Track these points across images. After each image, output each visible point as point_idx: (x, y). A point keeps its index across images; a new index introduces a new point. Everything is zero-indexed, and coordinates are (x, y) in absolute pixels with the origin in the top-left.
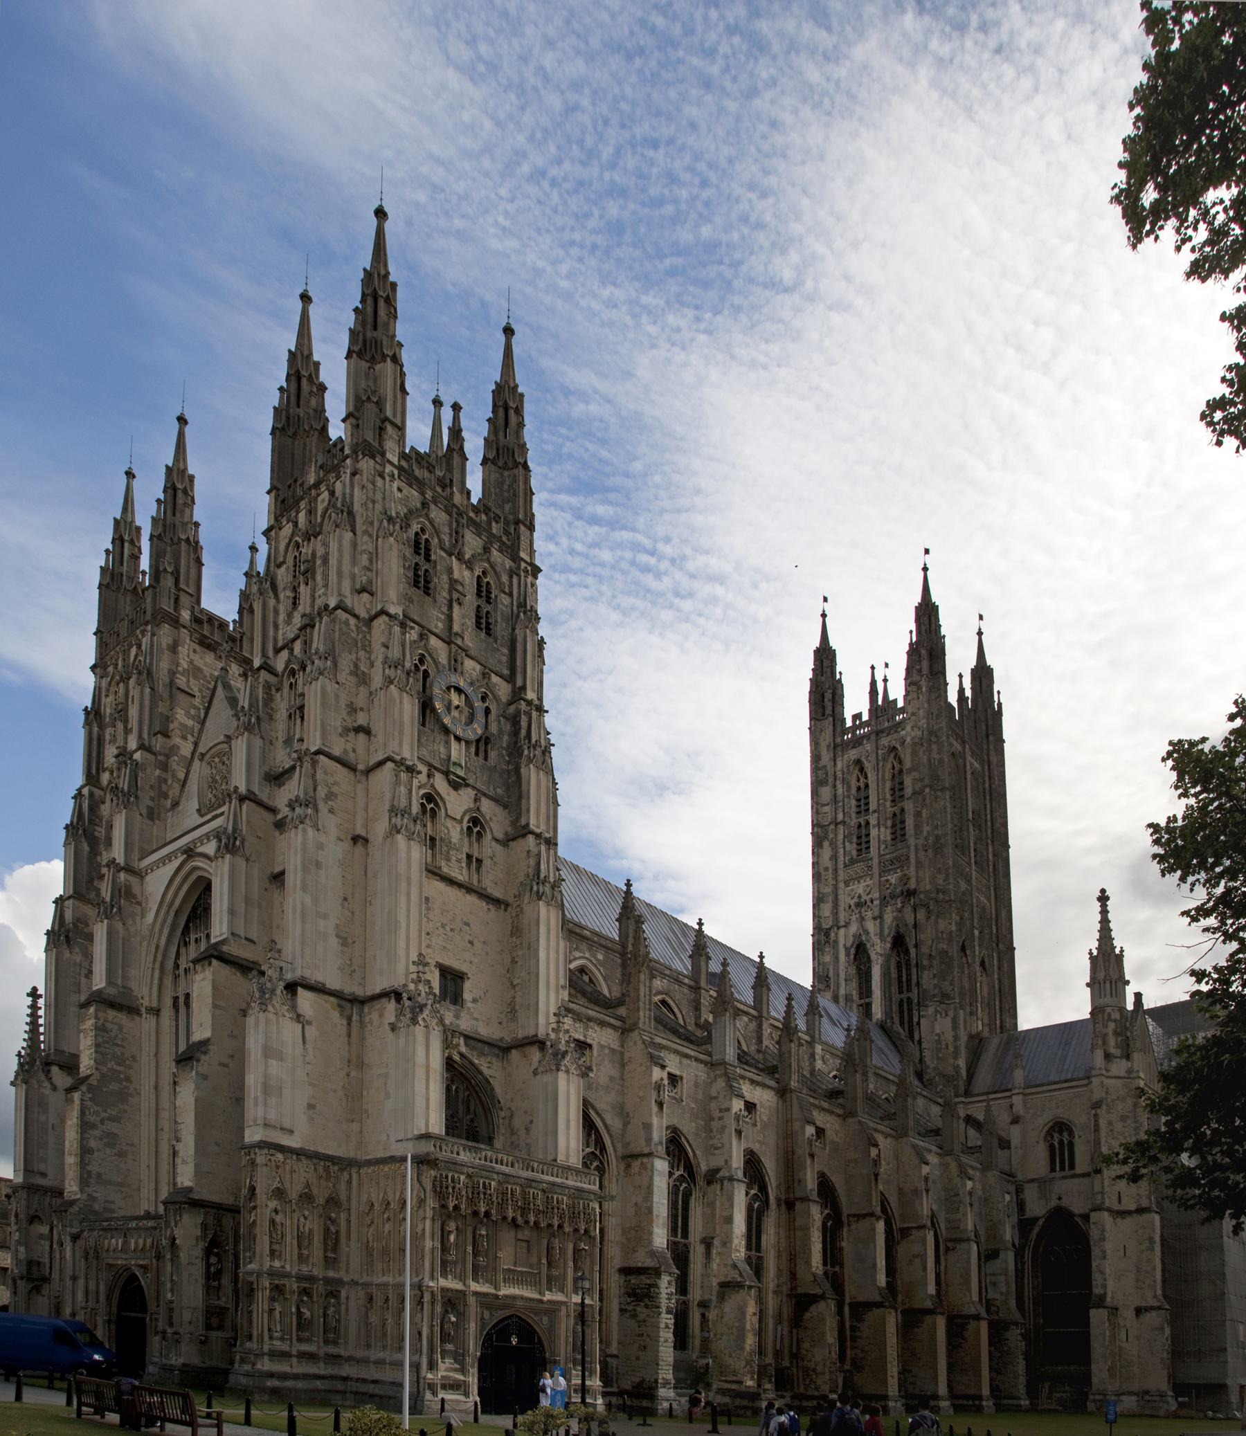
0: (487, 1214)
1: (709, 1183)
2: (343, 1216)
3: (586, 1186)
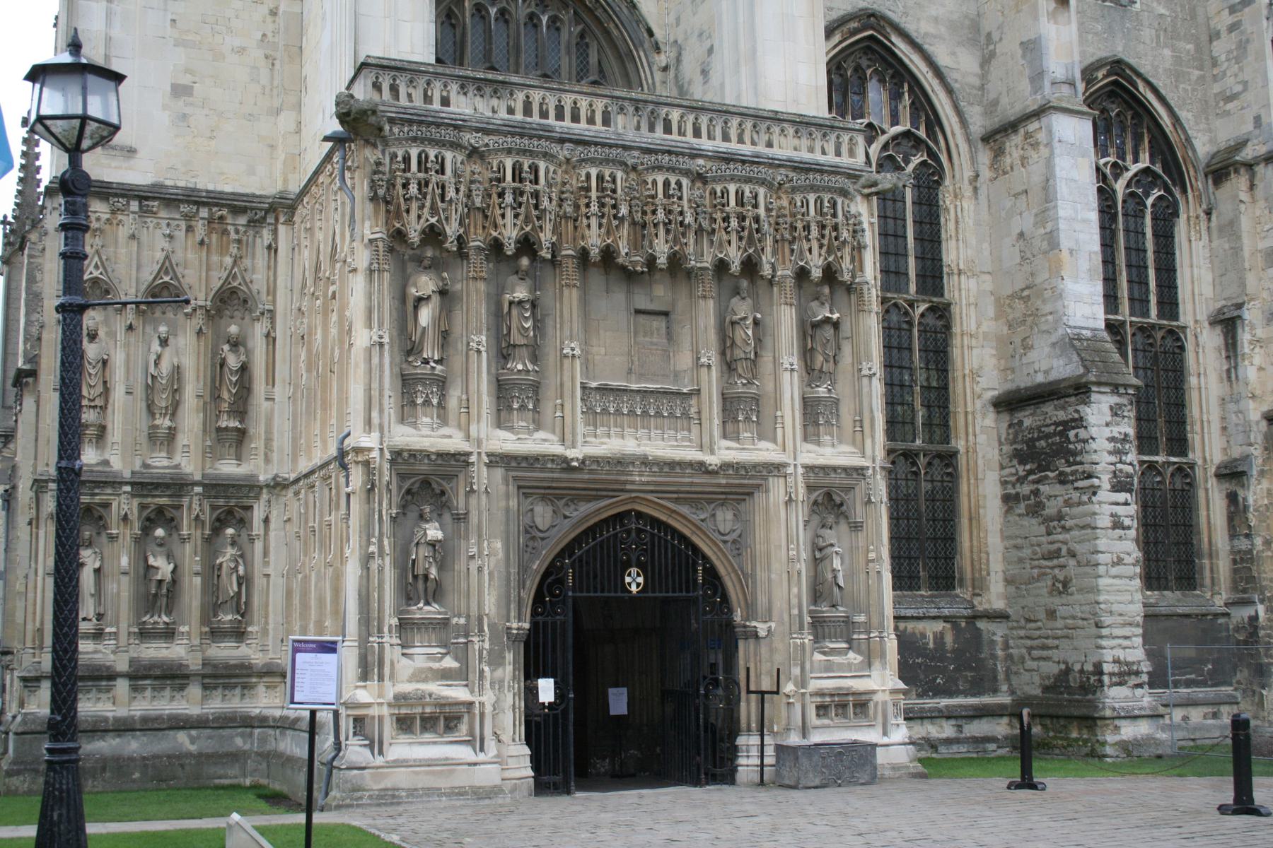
0: (527, 245)
1: (1220, 171)
2: (259, 329)
3: (831, 159)
